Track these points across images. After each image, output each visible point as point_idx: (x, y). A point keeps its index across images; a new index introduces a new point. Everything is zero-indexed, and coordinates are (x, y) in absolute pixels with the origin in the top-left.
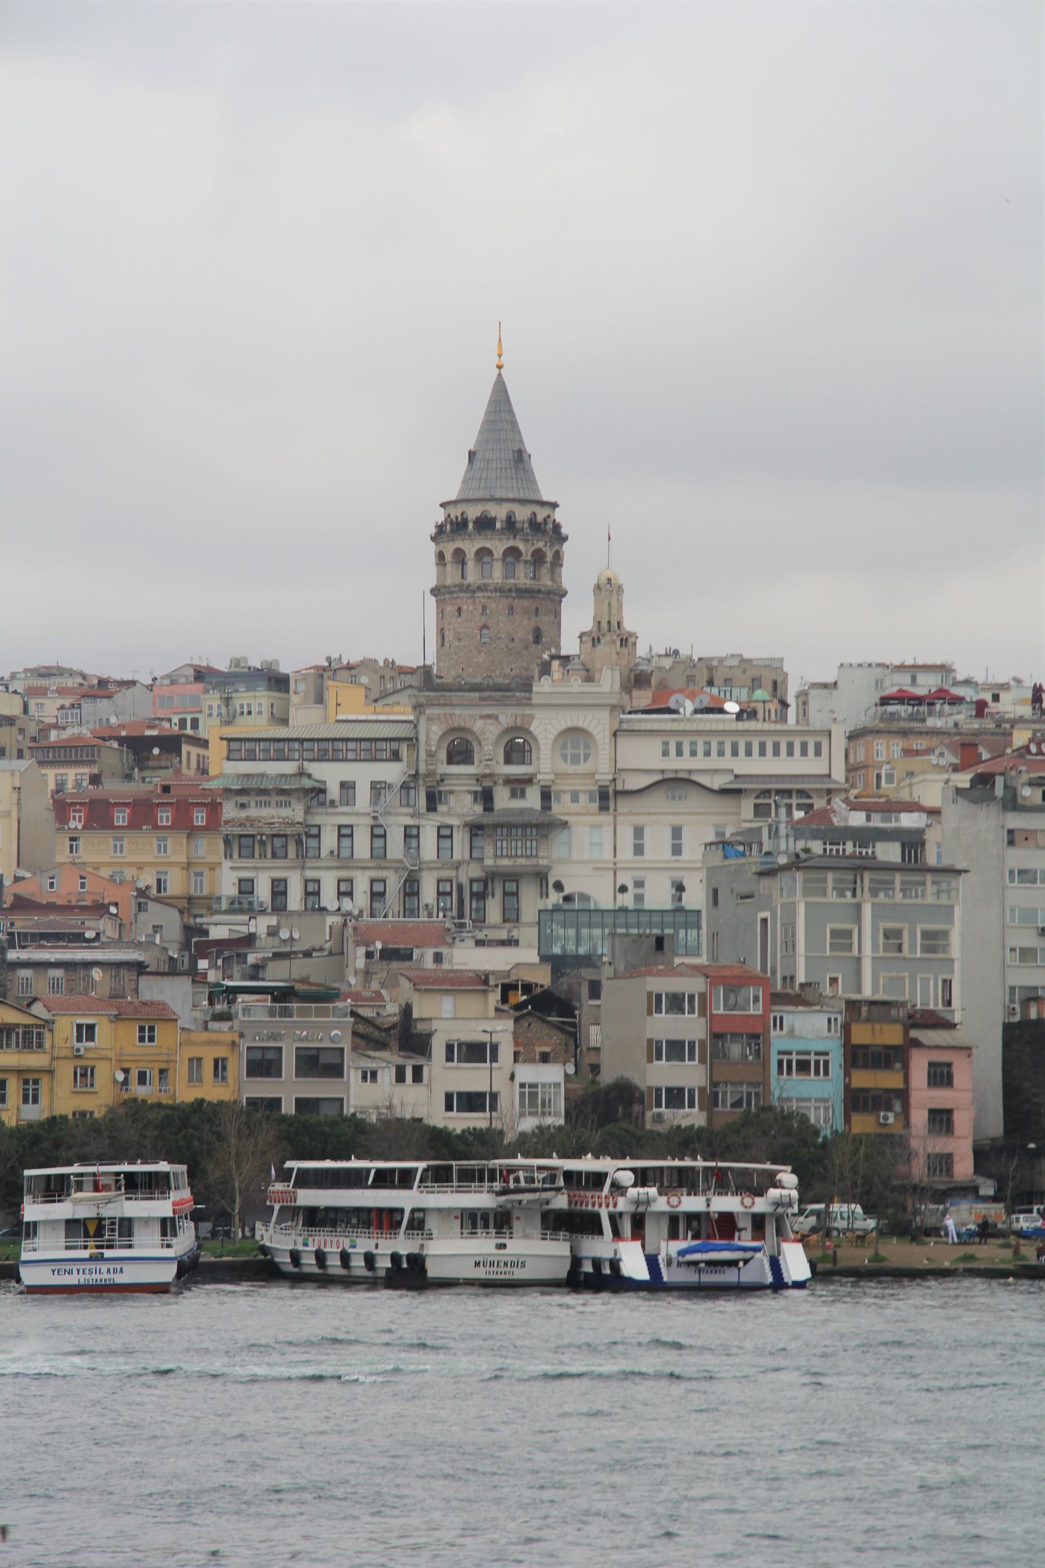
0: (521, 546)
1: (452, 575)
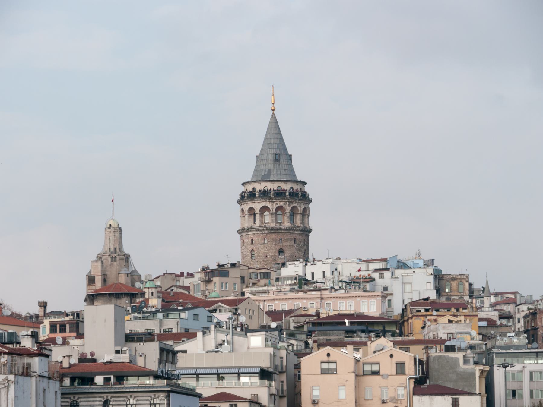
0: (269, 205)
1: (248, 222)
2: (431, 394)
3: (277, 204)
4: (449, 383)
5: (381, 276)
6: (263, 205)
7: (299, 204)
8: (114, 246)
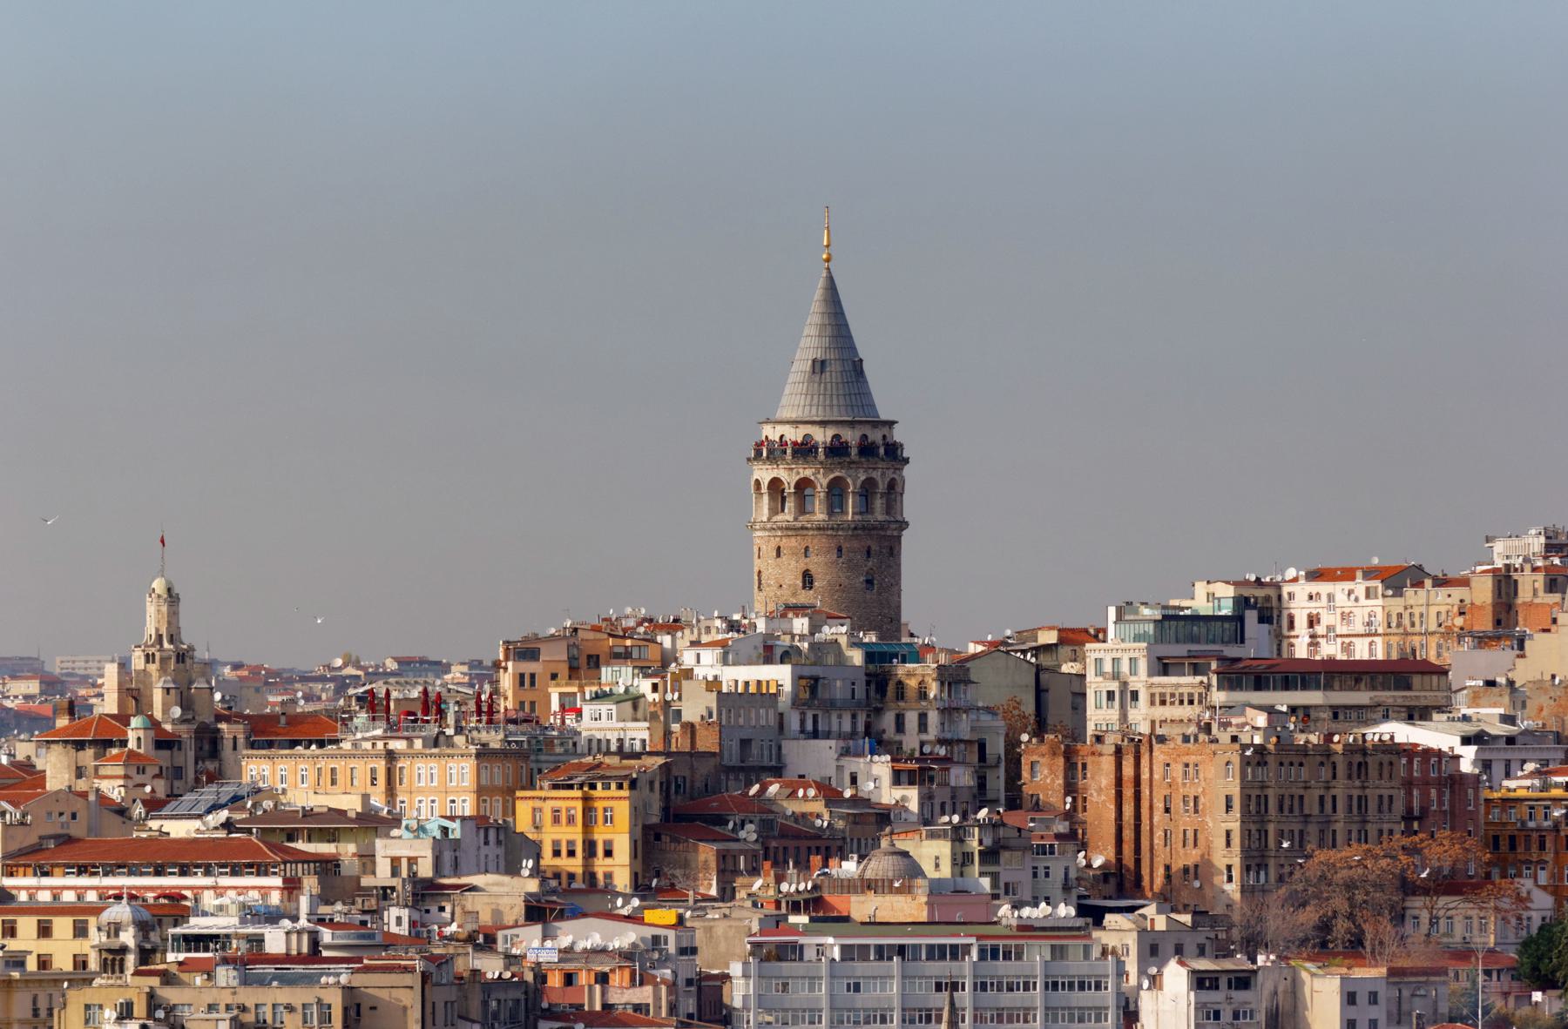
3: (798, 473)
6: (772, 476)
7: (852, 472)
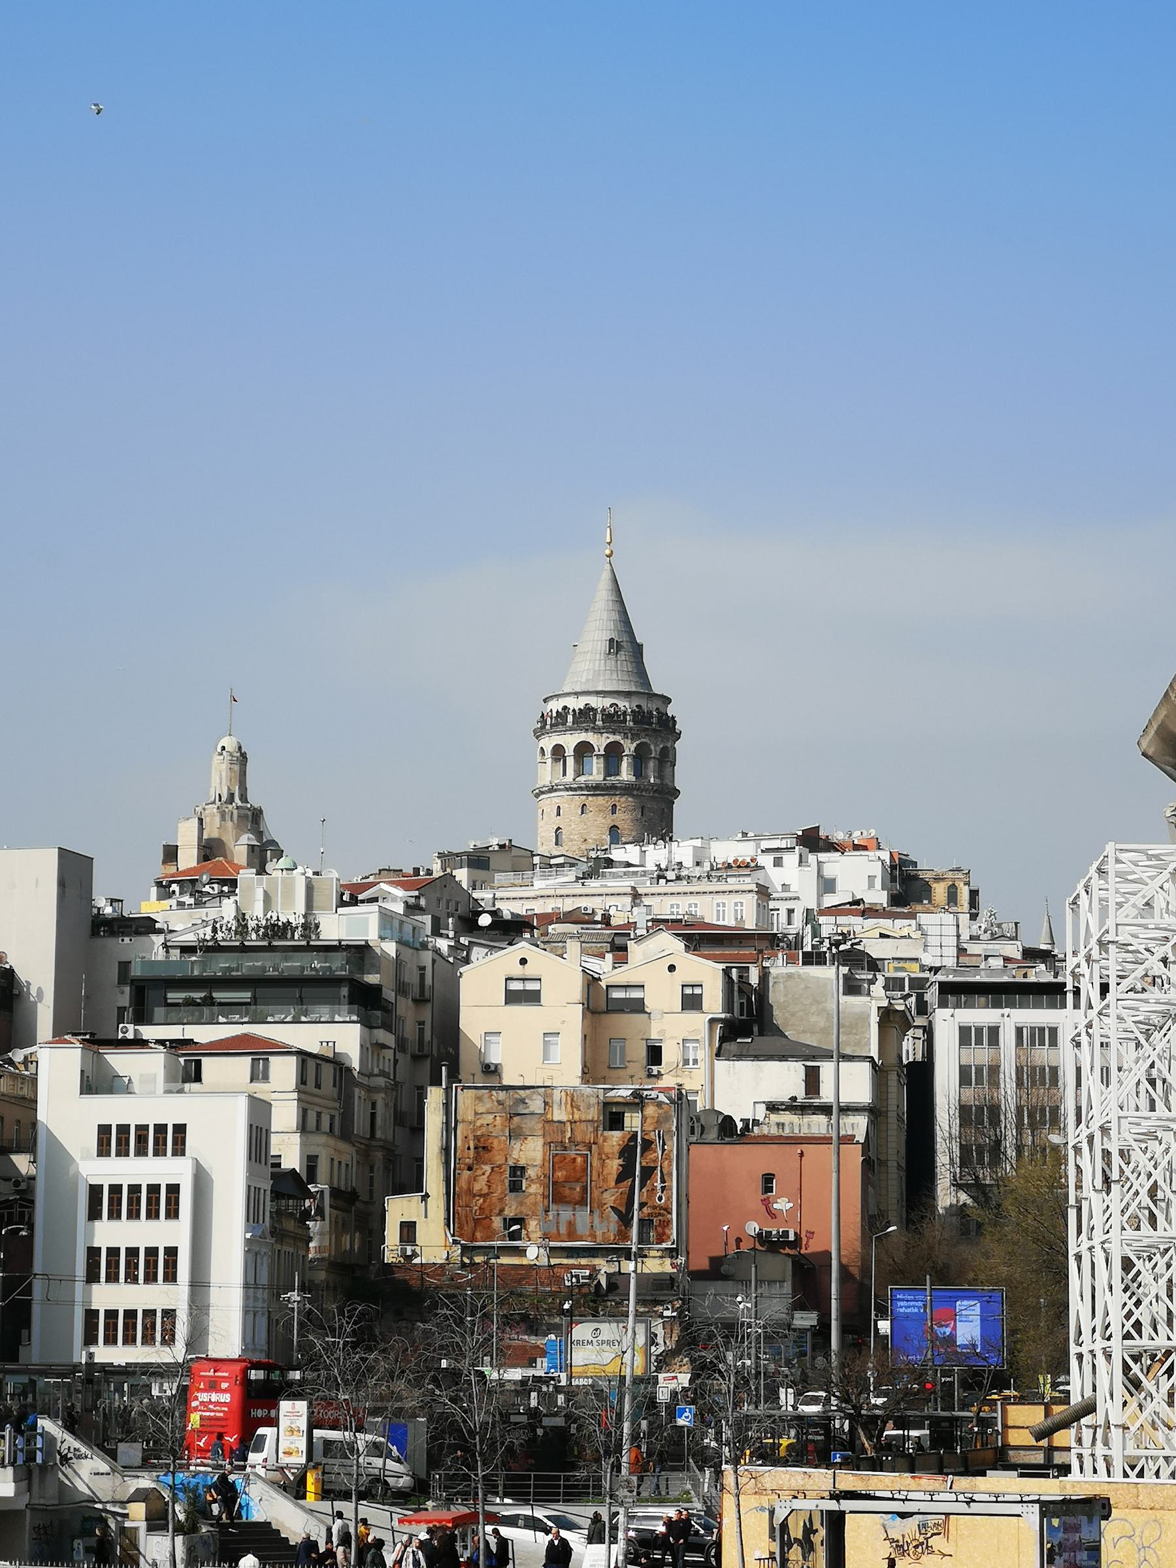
2: (757, 1057)
4: (809, 1034)
5: (778, 863)
8: (229, 789)
